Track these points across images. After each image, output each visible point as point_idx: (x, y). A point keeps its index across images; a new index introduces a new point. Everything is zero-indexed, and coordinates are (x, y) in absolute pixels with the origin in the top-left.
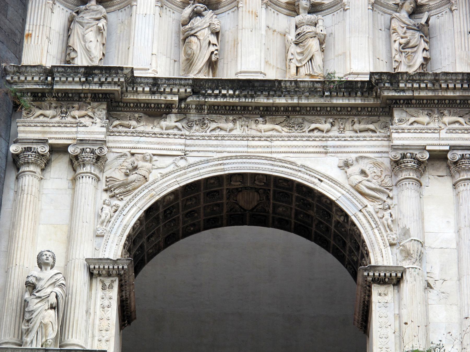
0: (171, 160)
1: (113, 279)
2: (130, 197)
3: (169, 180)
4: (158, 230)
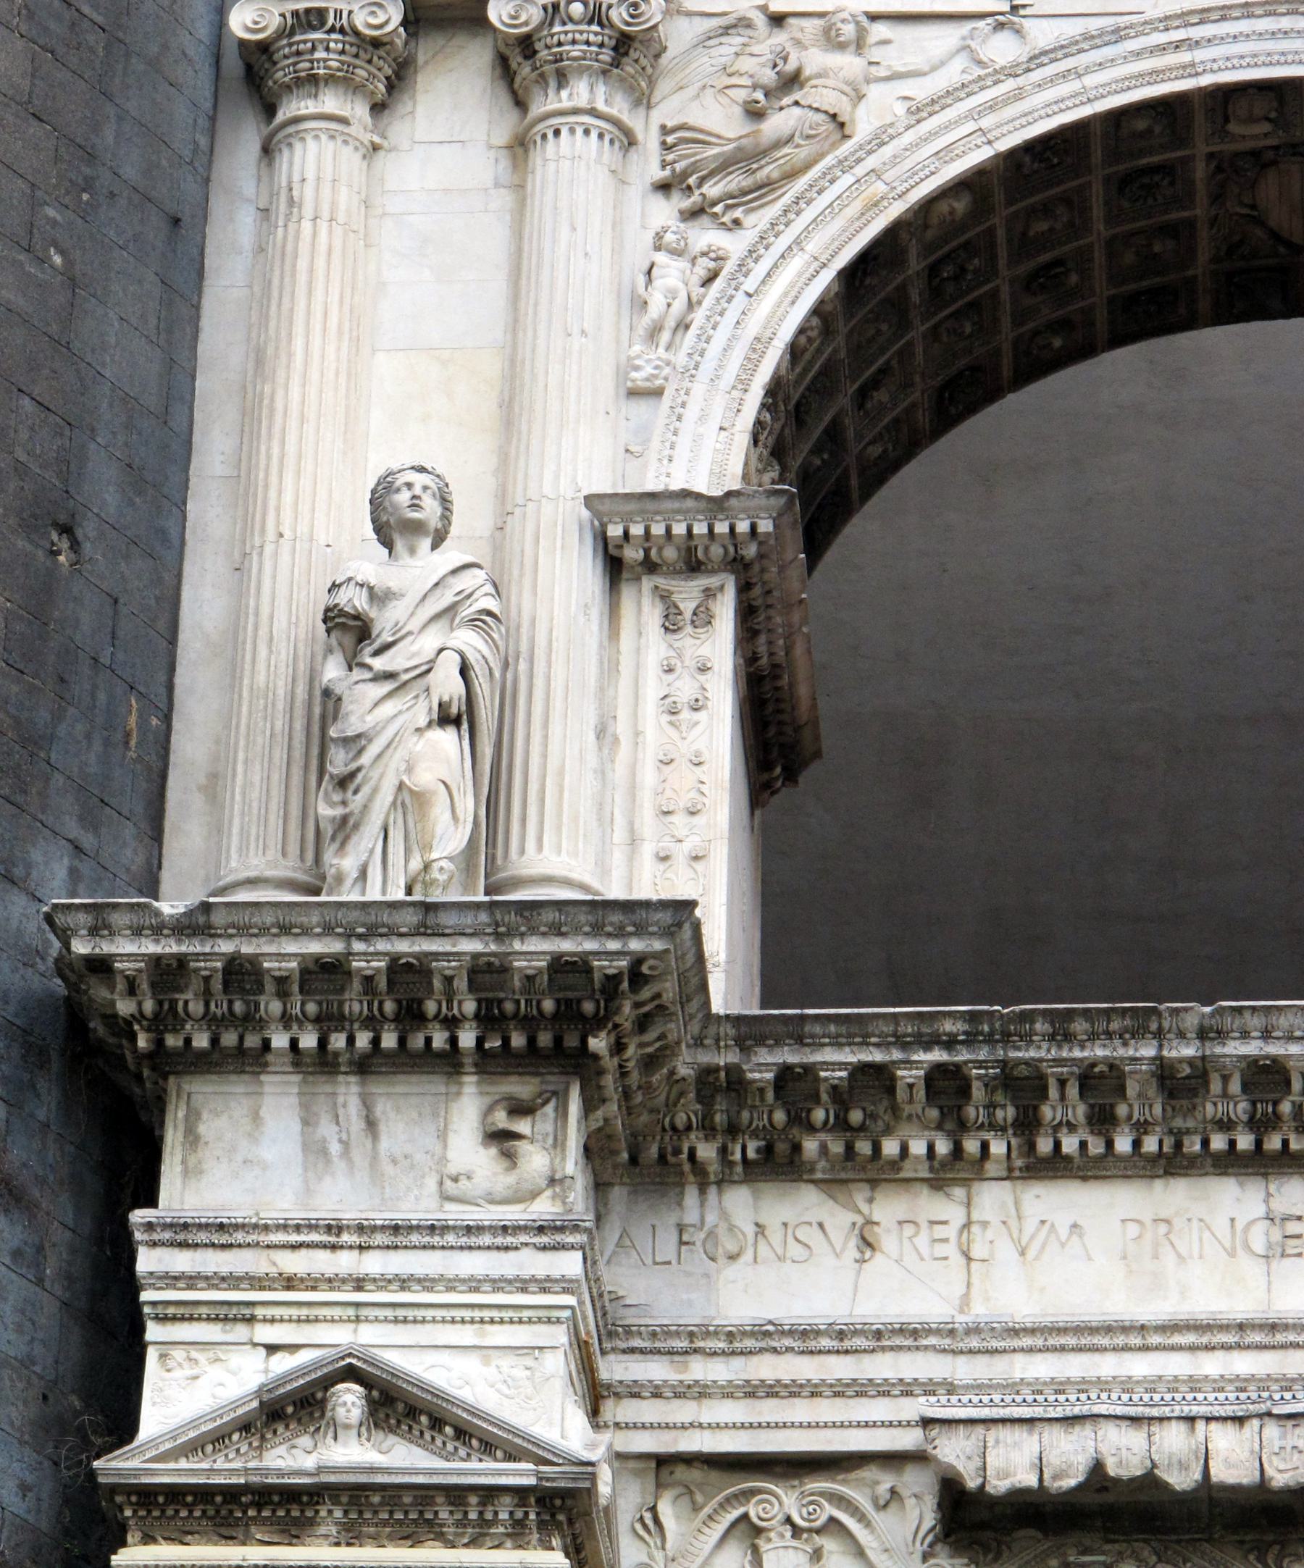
0: (950, 36)
1: (713, 581)
2: (773, 211)
3: (947, 128)
4: (905, 354)
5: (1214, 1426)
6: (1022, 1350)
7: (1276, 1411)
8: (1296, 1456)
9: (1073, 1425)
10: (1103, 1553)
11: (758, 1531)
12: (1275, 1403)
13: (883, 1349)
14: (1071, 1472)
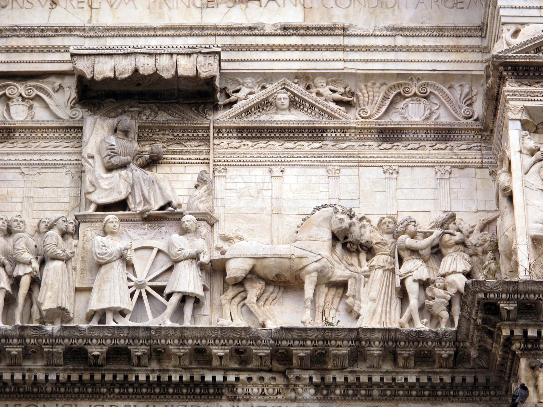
5: (179, 56)
6: (110, 36)
7: (203, 51)
8: (210, 66)
9: (127, 56)
10: (138, 107)
11: (9, 99)
12: (202, 48)
13: (58, 36)
14: (126, 72)
